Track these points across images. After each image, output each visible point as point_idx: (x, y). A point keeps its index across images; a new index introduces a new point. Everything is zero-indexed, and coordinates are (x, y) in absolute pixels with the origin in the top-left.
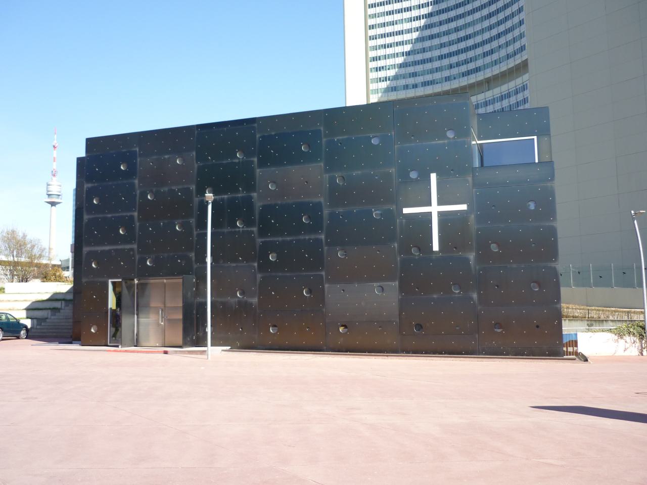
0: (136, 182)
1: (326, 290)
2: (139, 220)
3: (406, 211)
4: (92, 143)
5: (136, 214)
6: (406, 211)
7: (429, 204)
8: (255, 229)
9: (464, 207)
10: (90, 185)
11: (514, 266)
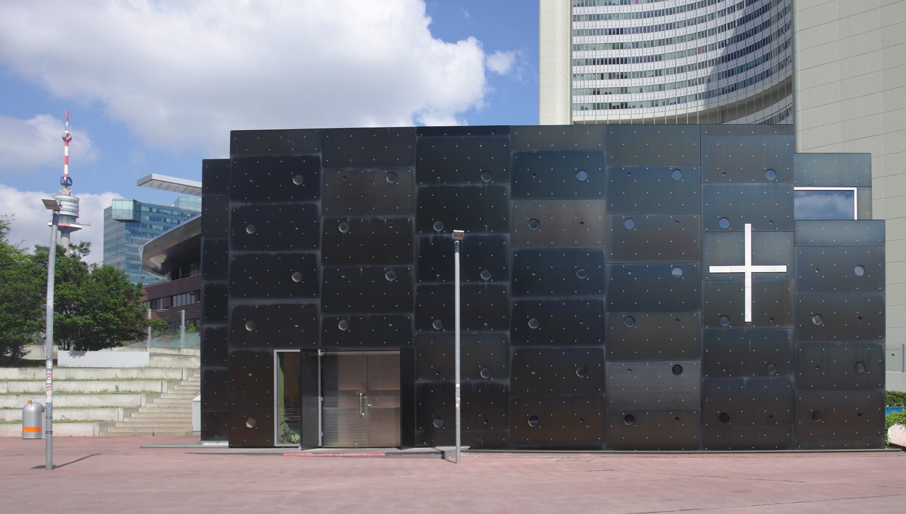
0: (319, 204)
1: (607, 369)
3: (713, 269)
4: (238, 138)
5: (319, 253)
6: (713, 269)
7: (743, 263)
8: (507, 284)
10: (239, 205)
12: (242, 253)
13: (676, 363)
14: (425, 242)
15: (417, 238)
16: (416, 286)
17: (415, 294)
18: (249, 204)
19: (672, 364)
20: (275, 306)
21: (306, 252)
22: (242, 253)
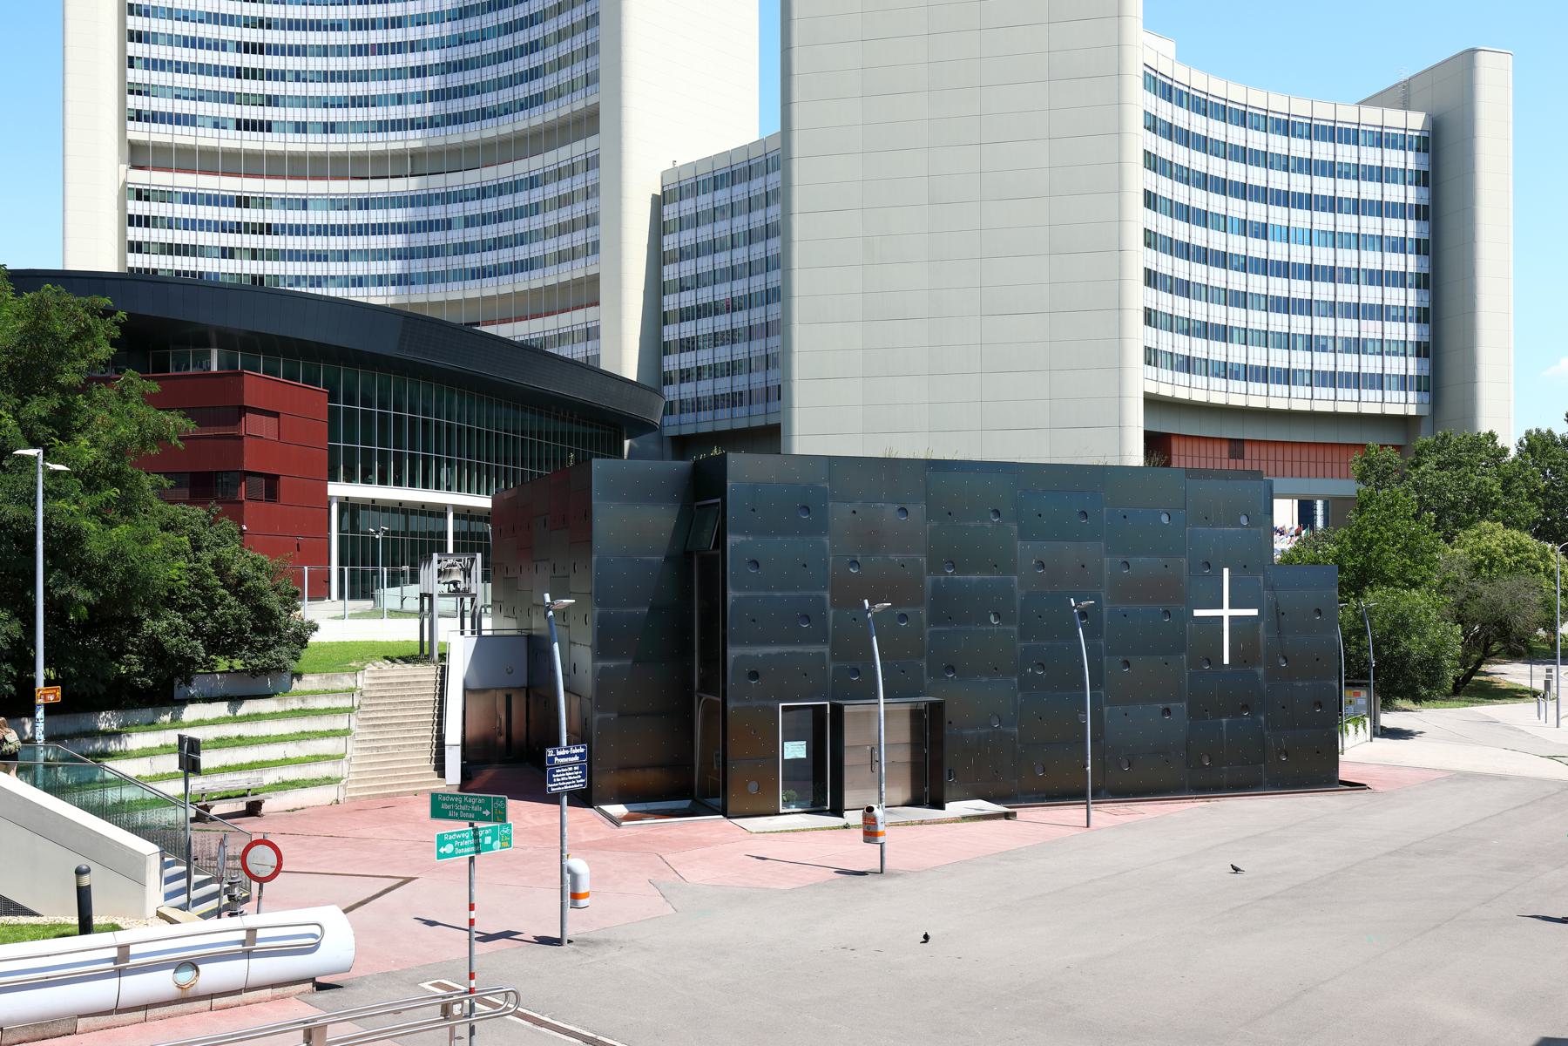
2: (833, 604)
5: (828, 596)
6: (1197, 613)
7: (1221, 607)
9: (1254, 612)
11: (1300, 684)
12: (742, 594)
13: (1165, 706)
14: (936, 584)
15: (929, 580)
16: (928, 631)
17: (927, 639)
18: (750, 539)
19: (1161, 706)
20: (780, 654)
21: (814, 593)
22: (742, 594)
